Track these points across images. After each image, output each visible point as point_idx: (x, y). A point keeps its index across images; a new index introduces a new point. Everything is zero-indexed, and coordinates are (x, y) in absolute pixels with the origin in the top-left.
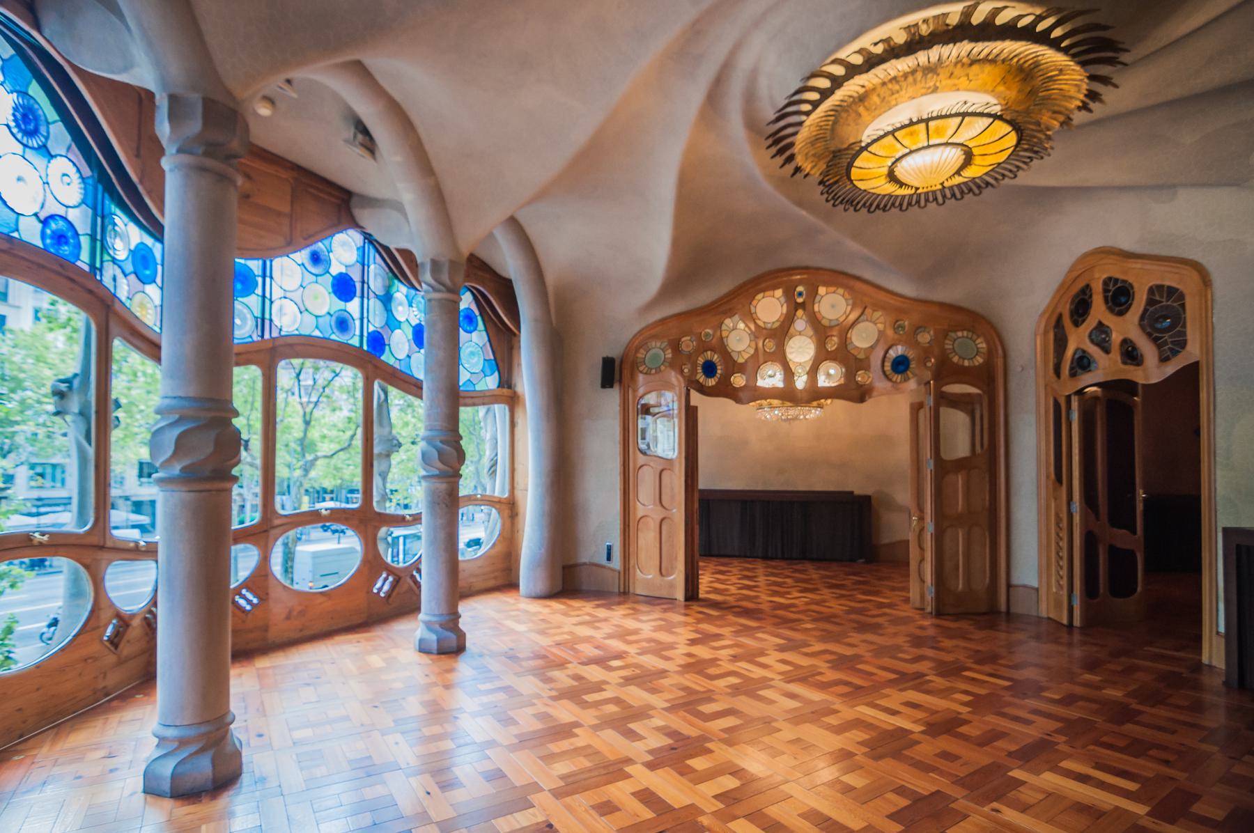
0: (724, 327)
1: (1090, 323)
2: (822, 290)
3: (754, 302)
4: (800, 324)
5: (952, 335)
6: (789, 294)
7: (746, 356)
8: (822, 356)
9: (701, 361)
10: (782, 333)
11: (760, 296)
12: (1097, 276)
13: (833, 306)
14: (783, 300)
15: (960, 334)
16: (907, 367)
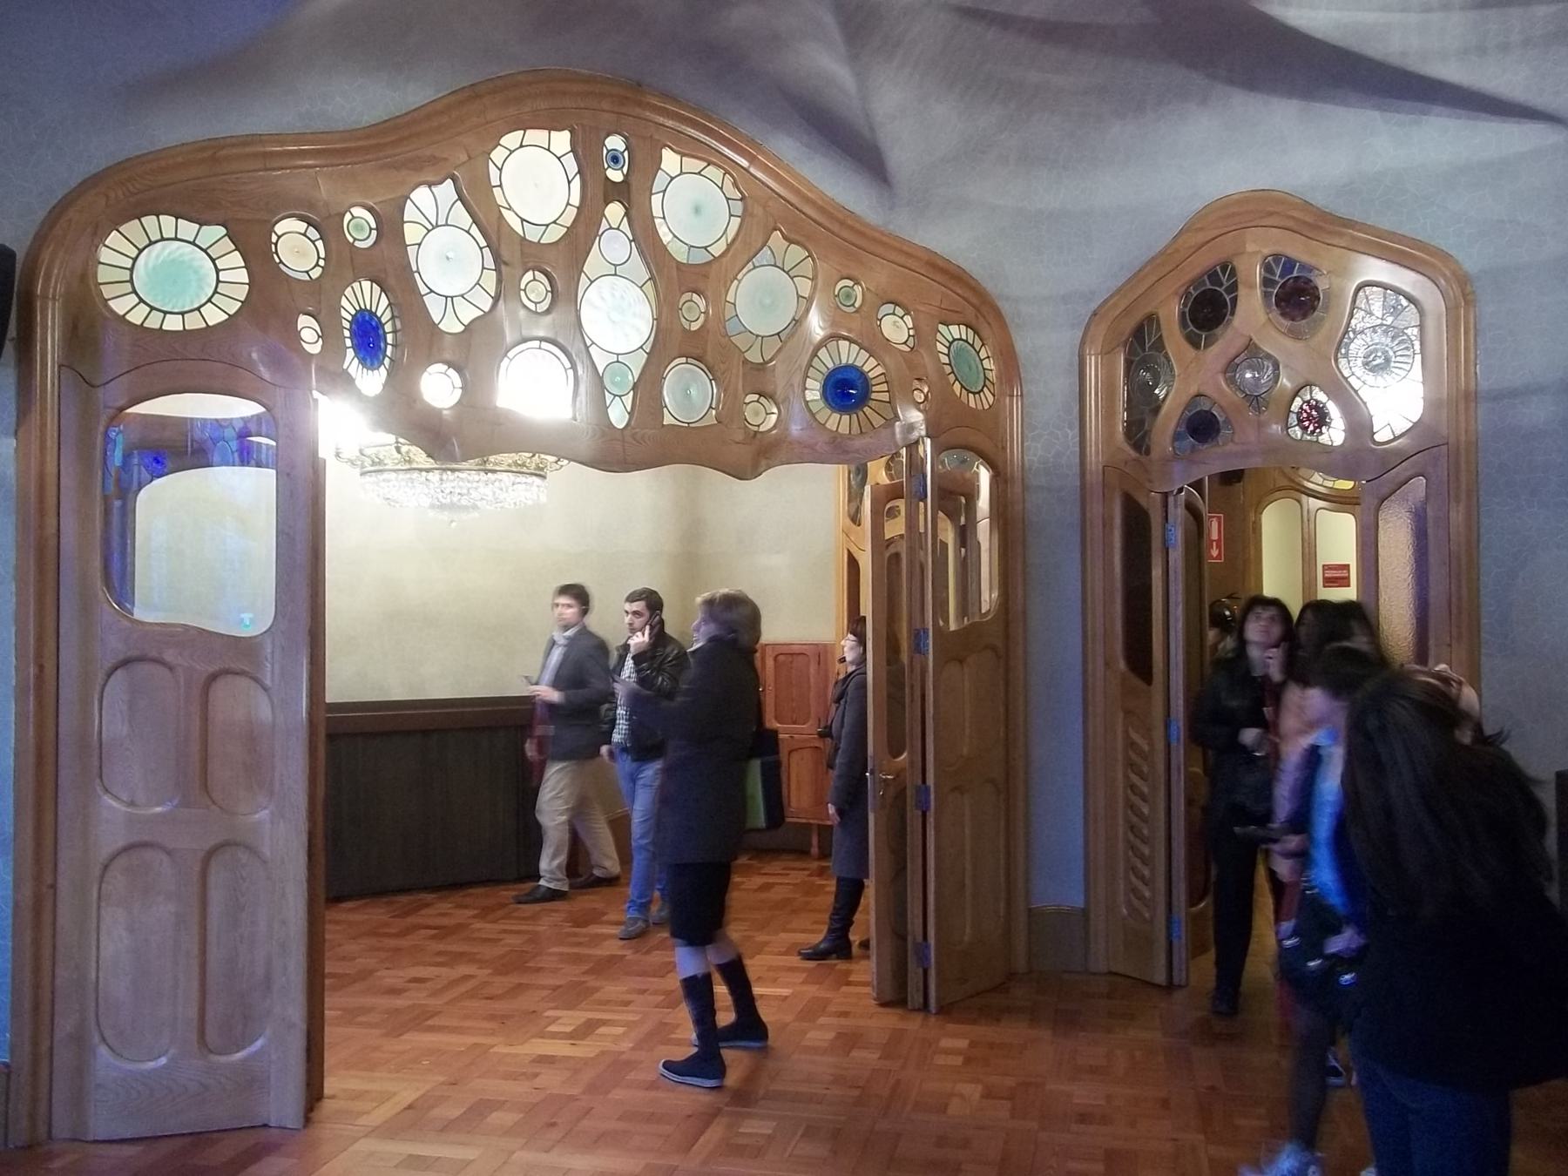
0: (410, 212)
1: (1227, 341)
2: (670, 160)
3: (497, 155)
4: (614, 241)
5: (942, 328)
6: (587, 155)
7: (468, 314)
8: (669, 343)
9: (348, 309)
10: (565, 260)
11: (511, 139)
12: (1250, 247)
13: (697, 210)
14: (570, 162)
15: (954, 329)
16: (864, 398)
